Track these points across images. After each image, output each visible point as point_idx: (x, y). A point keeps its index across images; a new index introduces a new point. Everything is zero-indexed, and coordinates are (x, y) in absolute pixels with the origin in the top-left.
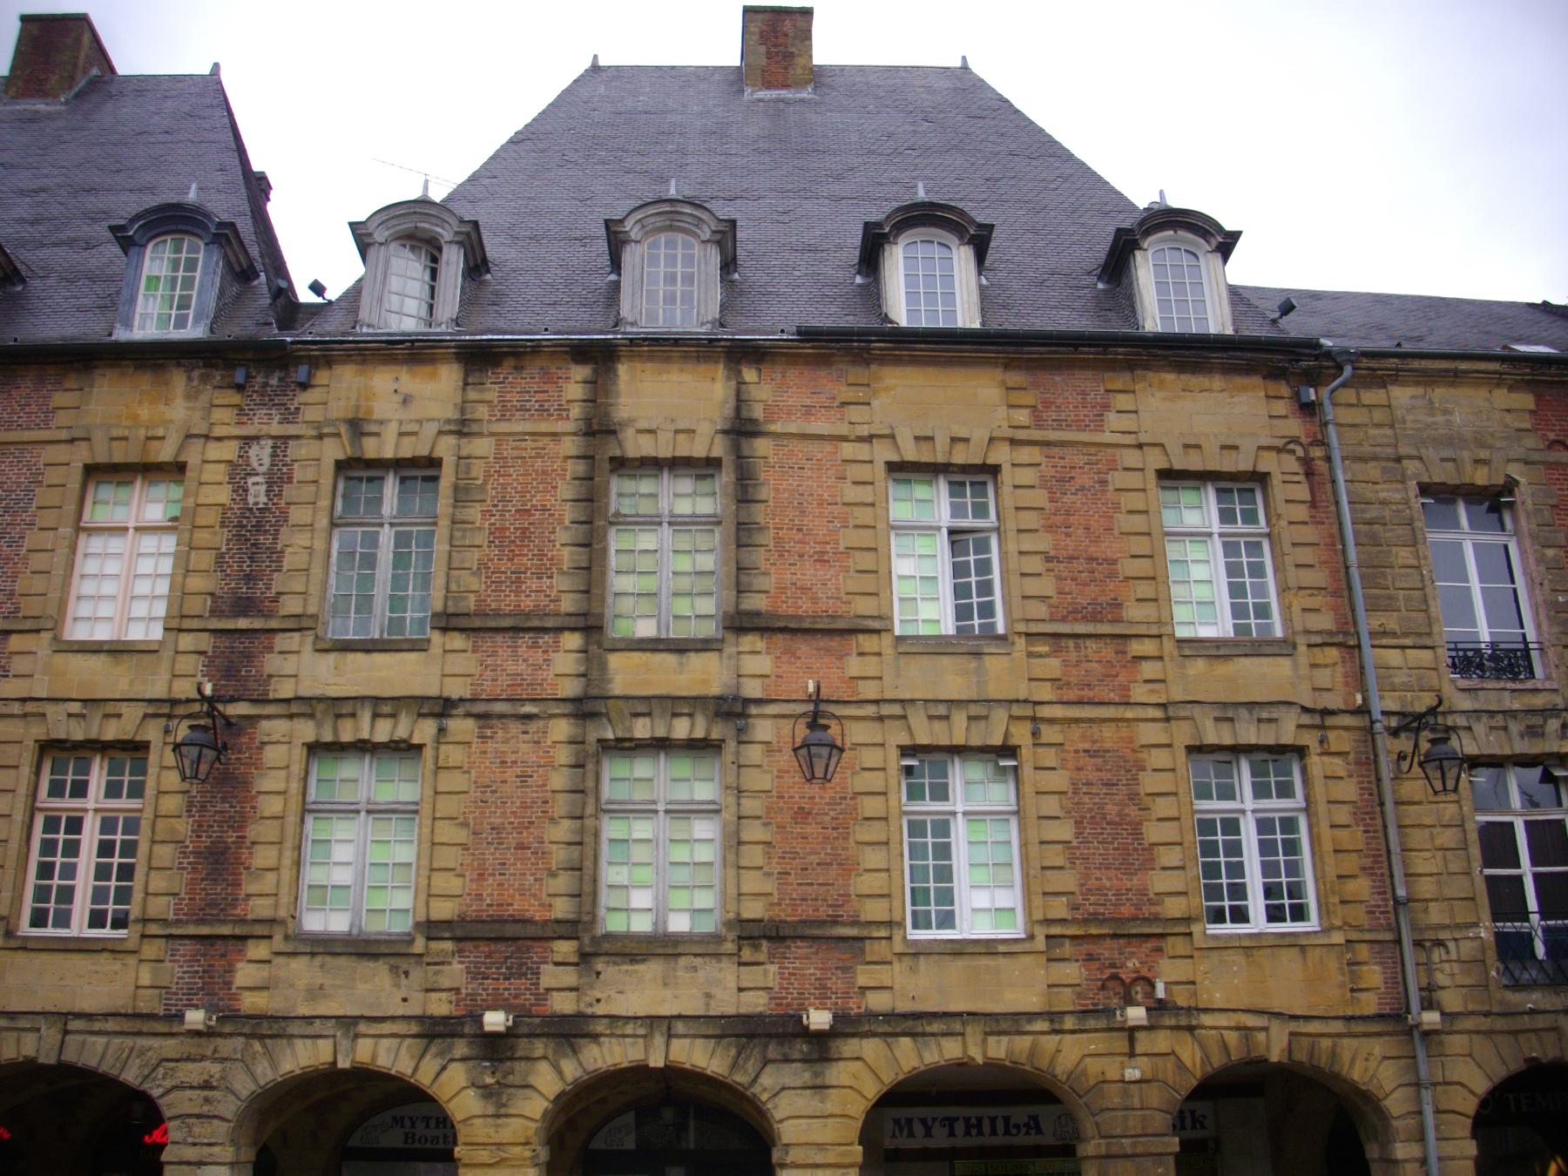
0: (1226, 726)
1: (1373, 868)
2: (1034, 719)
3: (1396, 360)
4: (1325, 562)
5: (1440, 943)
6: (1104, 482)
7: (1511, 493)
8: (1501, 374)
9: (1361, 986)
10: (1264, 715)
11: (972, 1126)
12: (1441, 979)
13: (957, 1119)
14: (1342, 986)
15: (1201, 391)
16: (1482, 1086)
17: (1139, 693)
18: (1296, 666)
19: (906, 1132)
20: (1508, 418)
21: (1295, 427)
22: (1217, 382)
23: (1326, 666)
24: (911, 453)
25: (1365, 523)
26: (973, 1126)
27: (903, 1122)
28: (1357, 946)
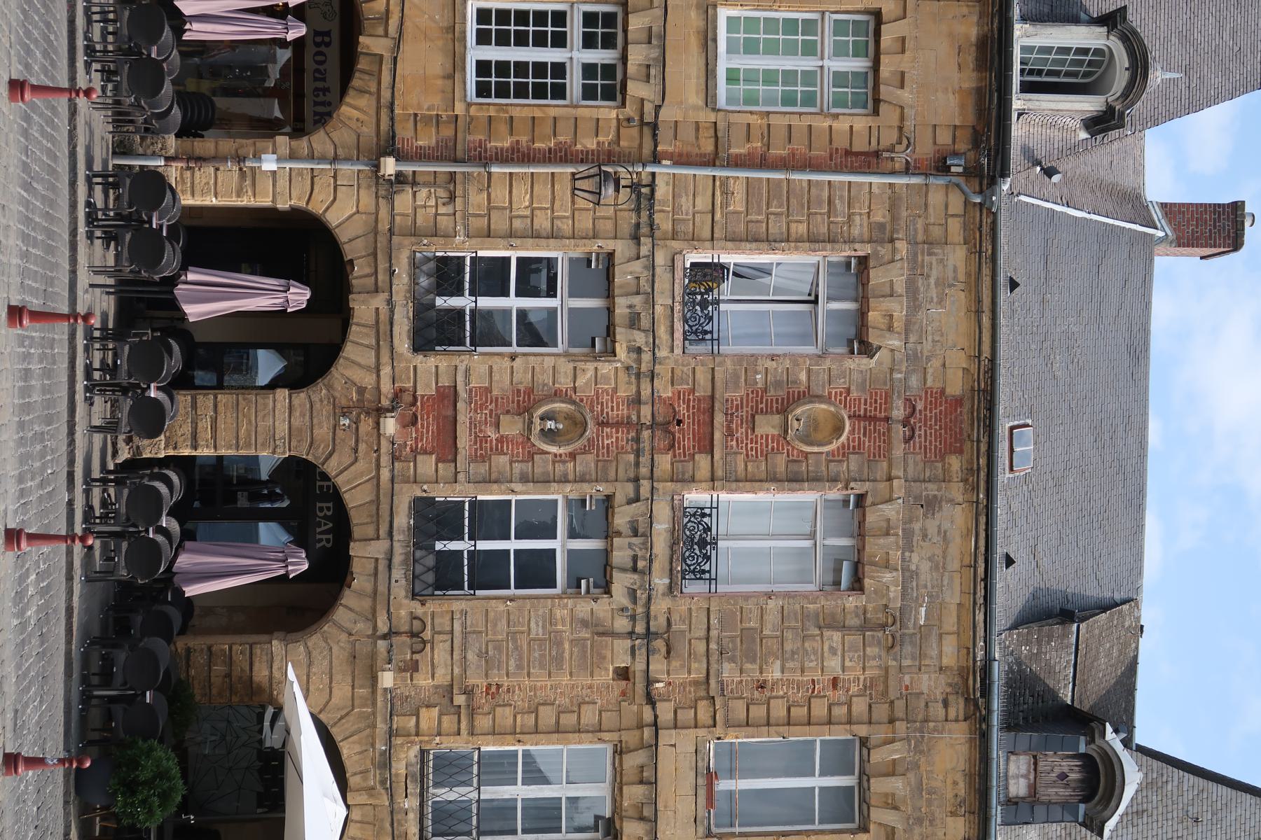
0: (644, 36)
1: (518, 152)
3: (990, 251)
4: (794, 155)
5: (452, 198)
9: (419, 124)
10: (653, 72)
12: (423, 193)
14: (419, 106)
16: (333, 219)
18: (696, 108)
20: (936, 363)
21: (925, 150)
23: (697, 138)
25: (829, 197)
28: (453, 126)
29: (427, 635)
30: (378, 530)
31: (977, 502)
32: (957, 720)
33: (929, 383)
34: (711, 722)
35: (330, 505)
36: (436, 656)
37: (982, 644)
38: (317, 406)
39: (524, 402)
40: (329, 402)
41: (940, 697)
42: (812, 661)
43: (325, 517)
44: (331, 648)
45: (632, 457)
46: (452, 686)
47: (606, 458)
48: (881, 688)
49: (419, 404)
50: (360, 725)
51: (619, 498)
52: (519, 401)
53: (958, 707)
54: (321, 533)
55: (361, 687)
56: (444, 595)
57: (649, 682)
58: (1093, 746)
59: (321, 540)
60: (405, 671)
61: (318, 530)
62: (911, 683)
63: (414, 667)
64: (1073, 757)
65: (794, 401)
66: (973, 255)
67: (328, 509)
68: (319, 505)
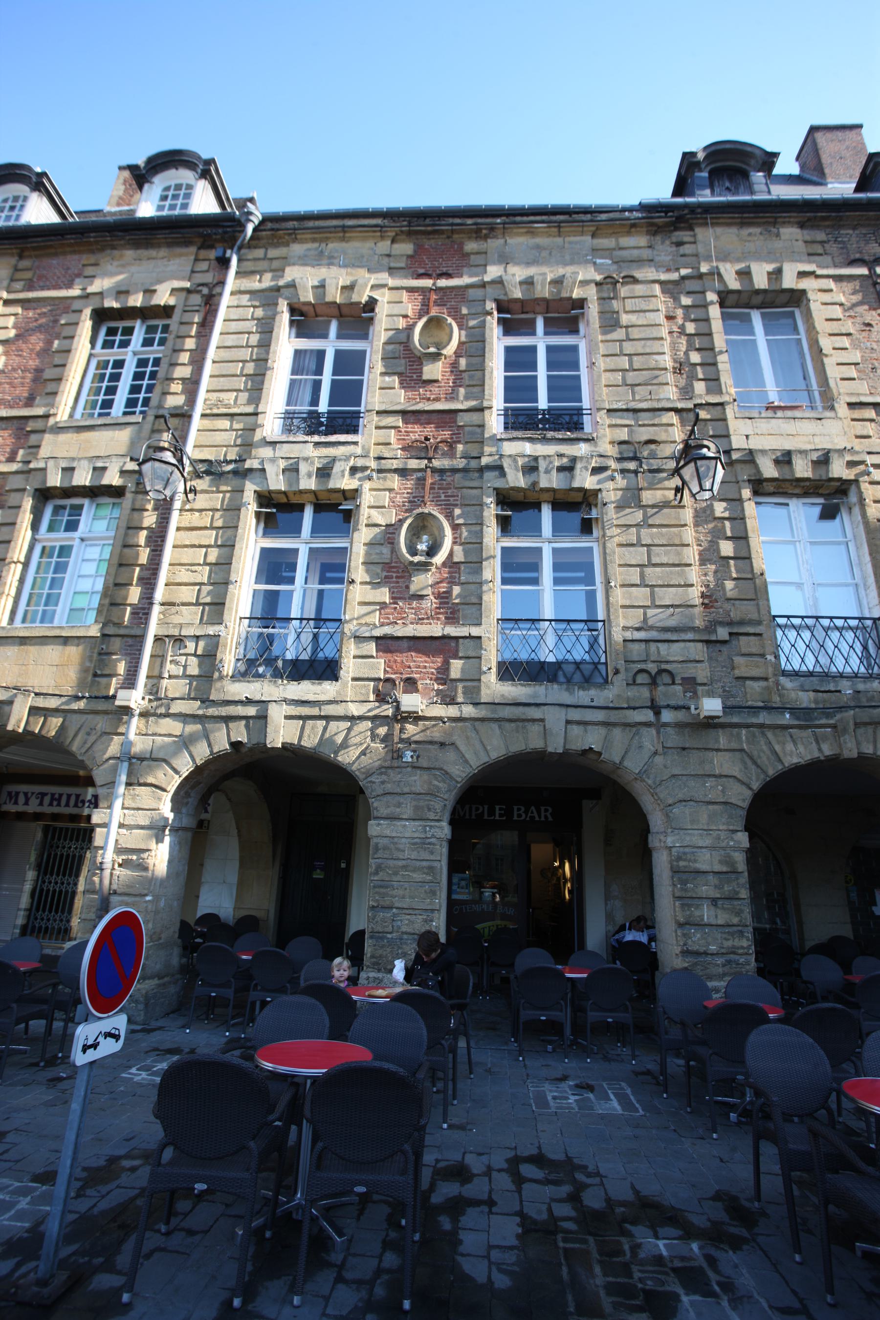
3: (295, 223)
6: (56, 321)
7: (372, 310)
8: (382, 227)
9: (105, 672)
11: (56, 799)
13: (46, 794)
15: (149, 259)
19: (13, 801)
22: (163, 252)
26: (56, 800)
27: (13, 794)
29: (652, 668)
30: (534, 720)
31: (504, 224)
32: (695, 236)
33: (403, 265)
35: (515, 808)
36: (676, 659)
37: (627, 213)
38: (389, 787)
39: (398, 572)
40: (385, 773)
41: (674, 248)
43: (526, 812)
44: (674, 776)
45: (458, 476)
46: (707, 642)
47: (459, 498)
49: (393, 676)
50: (762, 743)
51: (500, 484)
52: (397, 577)
53: (684, 235)
54: (540, 817)
55: (717, 741)
56: (605, 652)
58: (703, 166)
59: (546, 817)
60: (695, 693)
61: (537, 819)
62: (664, 267)
63: (691, 683)
65: (413, 353)
66: (298, 237)
67: (519, 810)
68: (515, 818)
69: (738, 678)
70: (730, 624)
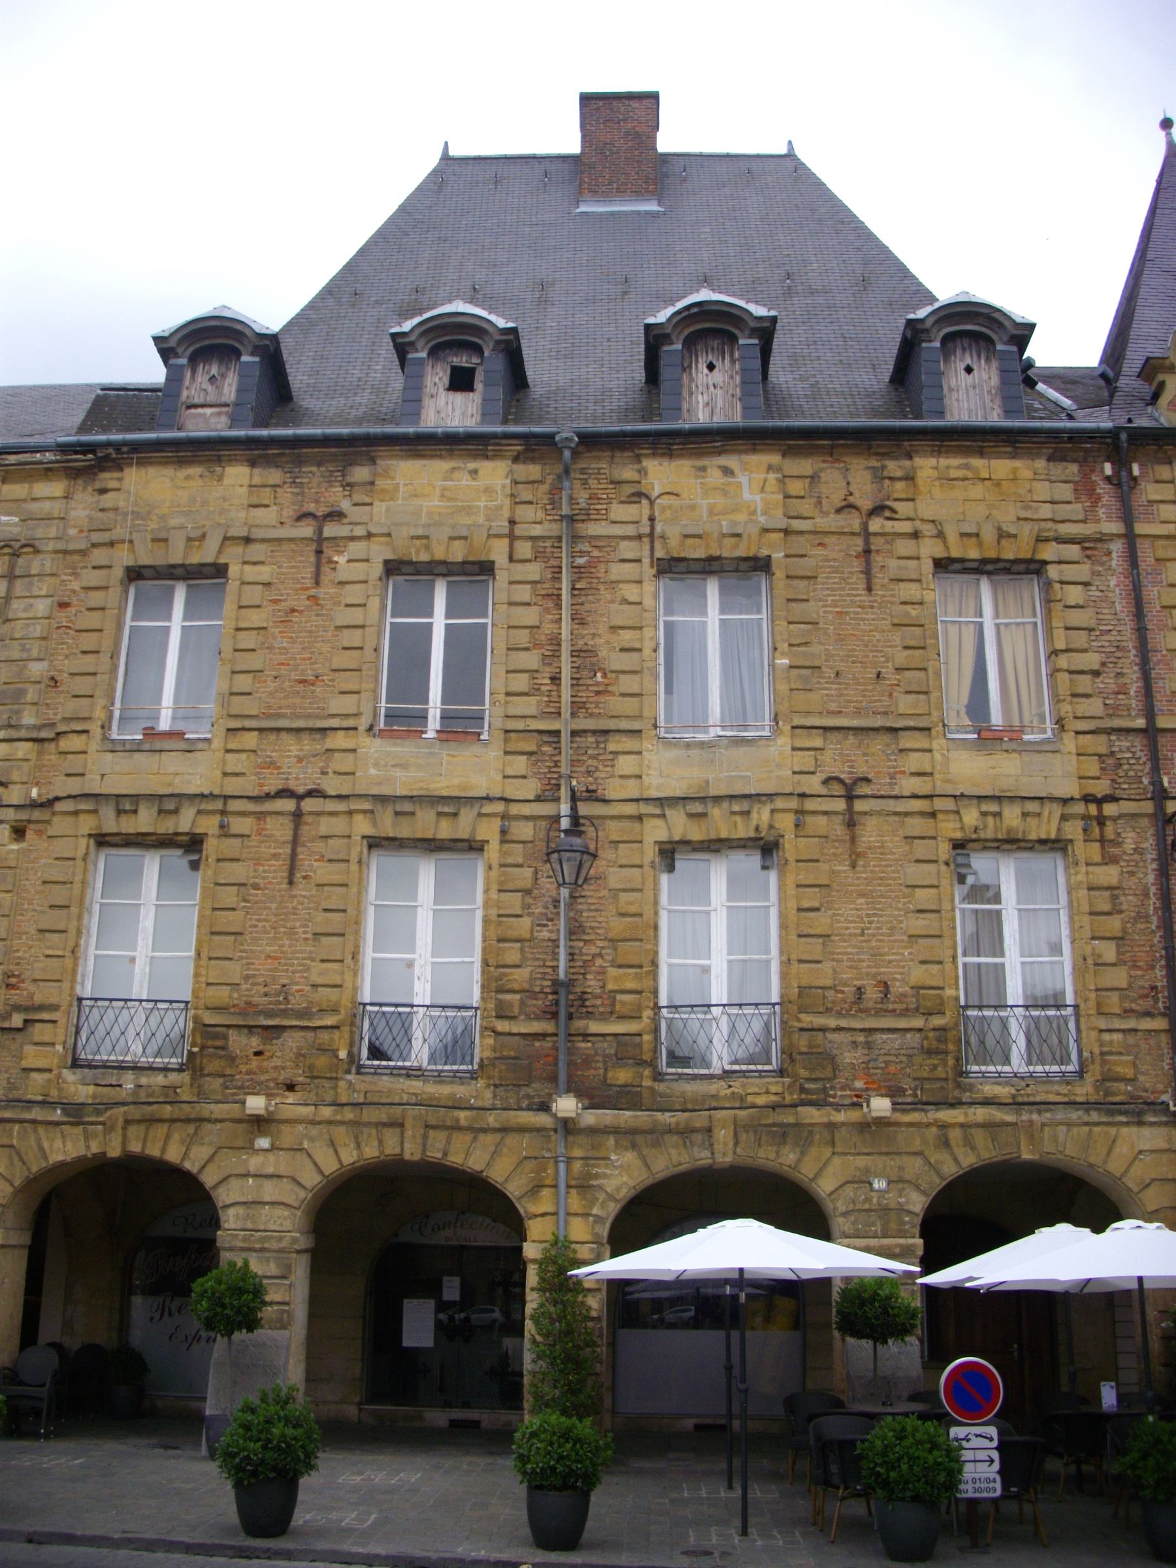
2: (223, 813)
17: (613, 789)
24: (146, 557)
34: (84, 736)
37: (38, 455)
41: (96, 497)
42: (35, 630)
48: (77, 557)
53: (108, 478)
57: (34, 805)
58: (180, 350)
64: (194, 372)
69: (24, 1069)
70: (27, 1009)
